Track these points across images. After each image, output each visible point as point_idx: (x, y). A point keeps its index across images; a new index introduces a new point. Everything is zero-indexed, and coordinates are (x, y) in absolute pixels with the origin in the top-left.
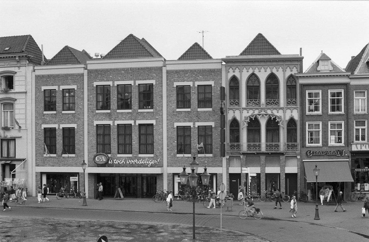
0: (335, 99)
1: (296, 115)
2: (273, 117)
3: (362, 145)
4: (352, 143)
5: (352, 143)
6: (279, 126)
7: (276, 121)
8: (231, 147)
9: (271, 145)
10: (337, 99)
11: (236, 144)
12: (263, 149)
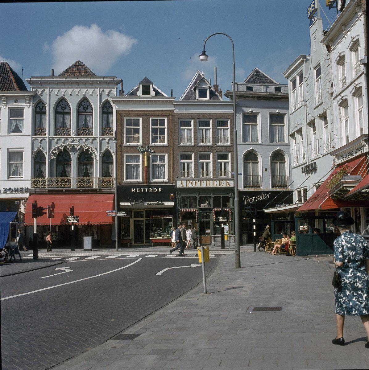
0: (157, 128)
1: (113, 147)
2: (63, 148)
3: (188, 182)
4: (176, 179)
5: (176, 179)
6: (92, 159)
7: (89, 153)
8: (35, 182)
9: (82, 180)
10: (159, 128)
11: (41, 179)
12: (74, 185)
